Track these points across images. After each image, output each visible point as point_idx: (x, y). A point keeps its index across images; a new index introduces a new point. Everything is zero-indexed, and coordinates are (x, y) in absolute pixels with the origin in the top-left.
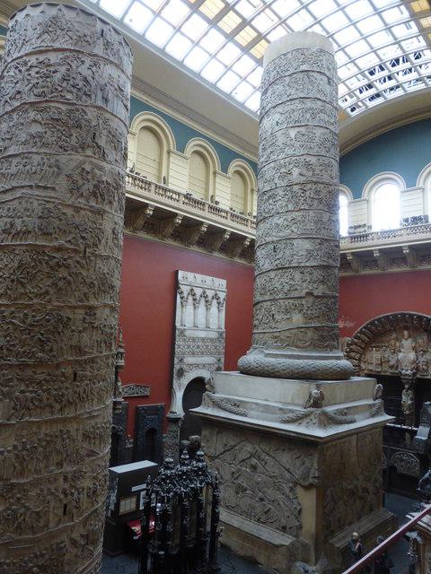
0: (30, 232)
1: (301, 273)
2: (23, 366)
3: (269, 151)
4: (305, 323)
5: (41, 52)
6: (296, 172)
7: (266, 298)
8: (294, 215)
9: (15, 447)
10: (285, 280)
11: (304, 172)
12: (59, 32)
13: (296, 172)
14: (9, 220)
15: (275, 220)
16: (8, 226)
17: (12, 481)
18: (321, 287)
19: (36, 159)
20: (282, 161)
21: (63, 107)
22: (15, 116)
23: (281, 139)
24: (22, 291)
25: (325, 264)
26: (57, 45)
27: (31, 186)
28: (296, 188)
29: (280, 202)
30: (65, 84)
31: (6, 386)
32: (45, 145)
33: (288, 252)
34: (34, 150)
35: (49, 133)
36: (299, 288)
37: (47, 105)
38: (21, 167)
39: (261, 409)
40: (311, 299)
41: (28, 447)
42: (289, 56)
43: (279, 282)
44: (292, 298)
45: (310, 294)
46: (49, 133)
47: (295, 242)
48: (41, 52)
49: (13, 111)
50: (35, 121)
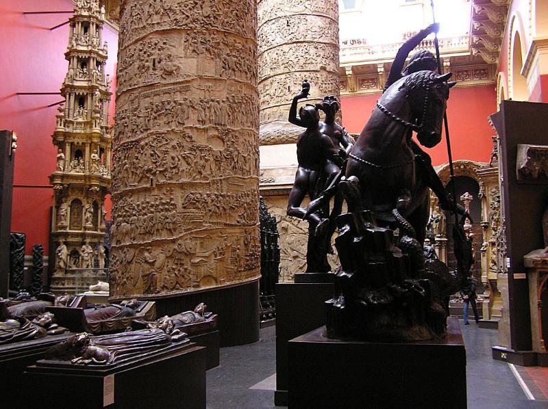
1: (316, 48)
9: (227, 98)
10: (300, 53)
17: (229, 127)
18: (332, 64)
33: (302, 28)
36: (314, 61)
40: (324, 74)
41: (237, 101)
43: (293, 54)
44: (308, 71)
45: (323, 68)
47: (308, 17)
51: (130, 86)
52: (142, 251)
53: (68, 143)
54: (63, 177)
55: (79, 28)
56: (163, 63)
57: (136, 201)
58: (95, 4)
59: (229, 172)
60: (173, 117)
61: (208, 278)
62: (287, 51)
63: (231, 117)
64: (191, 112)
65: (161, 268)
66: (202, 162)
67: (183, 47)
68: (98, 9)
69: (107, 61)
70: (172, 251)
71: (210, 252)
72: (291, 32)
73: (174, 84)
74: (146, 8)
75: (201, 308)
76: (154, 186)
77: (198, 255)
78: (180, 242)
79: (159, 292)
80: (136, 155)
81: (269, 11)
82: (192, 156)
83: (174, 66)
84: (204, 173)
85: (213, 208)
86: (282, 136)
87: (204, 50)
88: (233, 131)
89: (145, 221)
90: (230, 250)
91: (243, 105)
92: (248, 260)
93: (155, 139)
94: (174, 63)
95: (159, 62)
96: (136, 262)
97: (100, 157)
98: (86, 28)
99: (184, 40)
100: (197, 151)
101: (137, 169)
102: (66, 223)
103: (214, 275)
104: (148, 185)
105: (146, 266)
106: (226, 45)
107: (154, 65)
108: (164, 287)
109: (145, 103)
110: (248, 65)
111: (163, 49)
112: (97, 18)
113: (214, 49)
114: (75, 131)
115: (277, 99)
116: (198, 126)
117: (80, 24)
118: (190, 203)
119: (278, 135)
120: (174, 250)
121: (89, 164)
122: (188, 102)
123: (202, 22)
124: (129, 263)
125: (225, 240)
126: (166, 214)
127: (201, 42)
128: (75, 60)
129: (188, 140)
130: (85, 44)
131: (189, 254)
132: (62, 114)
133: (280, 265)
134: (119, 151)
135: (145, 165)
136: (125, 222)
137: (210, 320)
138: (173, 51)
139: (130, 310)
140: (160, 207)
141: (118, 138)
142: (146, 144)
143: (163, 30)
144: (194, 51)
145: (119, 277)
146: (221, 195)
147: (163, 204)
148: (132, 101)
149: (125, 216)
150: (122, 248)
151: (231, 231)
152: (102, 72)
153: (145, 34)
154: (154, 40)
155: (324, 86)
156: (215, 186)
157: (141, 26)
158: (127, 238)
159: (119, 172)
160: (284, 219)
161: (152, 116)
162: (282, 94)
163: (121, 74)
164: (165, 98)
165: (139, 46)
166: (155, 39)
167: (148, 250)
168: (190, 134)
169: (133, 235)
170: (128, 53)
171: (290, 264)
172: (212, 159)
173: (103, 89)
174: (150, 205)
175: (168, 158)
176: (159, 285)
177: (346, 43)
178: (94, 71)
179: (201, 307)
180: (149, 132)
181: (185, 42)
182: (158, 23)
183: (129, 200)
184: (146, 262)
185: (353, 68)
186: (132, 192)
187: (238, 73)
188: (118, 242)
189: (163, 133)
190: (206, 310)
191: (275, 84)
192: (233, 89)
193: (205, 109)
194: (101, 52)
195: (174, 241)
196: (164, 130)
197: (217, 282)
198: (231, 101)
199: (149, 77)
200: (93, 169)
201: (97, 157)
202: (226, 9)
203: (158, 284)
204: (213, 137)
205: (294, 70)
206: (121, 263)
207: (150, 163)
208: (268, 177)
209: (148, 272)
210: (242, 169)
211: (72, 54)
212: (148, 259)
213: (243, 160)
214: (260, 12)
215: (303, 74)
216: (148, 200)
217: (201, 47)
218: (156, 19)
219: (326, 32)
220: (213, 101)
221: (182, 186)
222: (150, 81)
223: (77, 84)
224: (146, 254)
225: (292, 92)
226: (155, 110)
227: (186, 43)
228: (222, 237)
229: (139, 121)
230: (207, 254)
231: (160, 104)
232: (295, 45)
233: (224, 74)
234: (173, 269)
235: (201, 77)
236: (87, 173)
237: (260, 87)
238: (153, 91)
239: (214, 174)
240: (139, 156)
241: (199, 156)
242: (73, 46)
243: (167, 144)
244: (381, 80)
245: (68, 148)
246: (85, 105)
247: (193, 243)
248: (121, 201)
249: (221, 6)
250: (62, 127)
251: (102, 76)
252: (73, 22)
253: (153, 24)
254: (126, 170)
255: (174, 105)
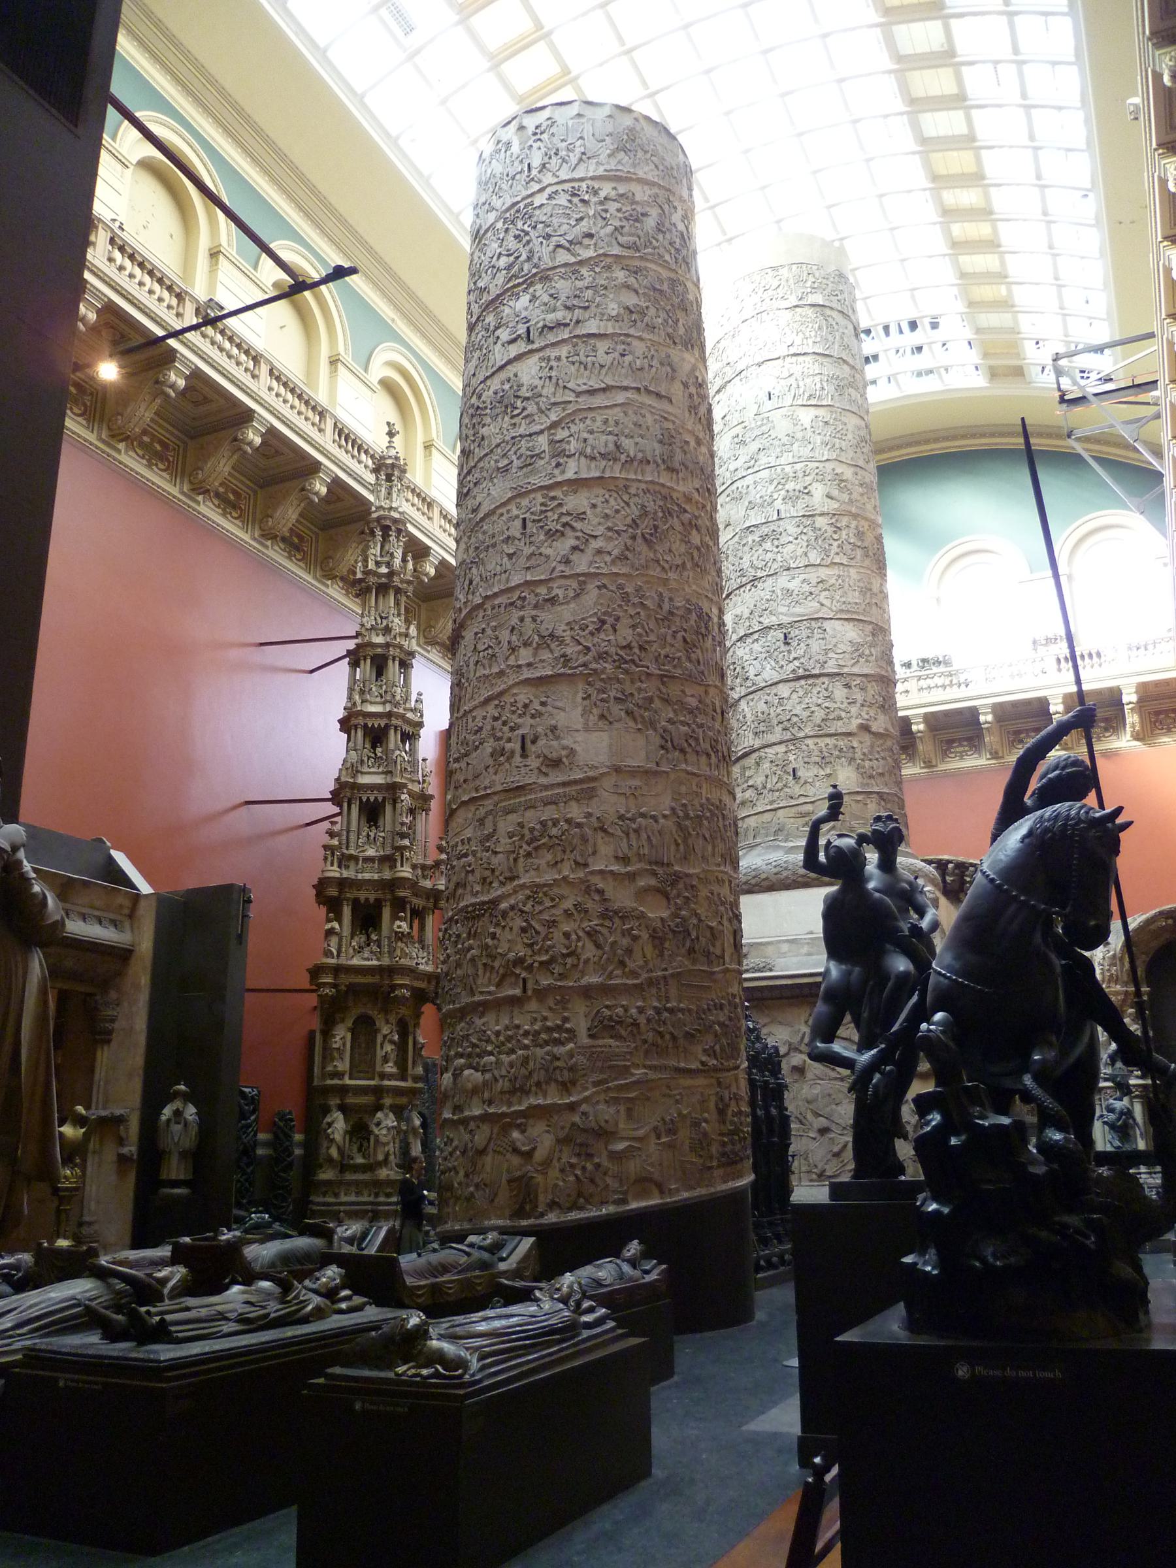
0: (648, 462)
1: (847, 686)
2: (664, 678)
3: (754, 447)
4: (863, 785)
5: (618, 179)
6: (818, 490)
7: (771, 738)
8: (823, 573)
9: (673, 809)
10: (813, 699)
11: (835, 493)
12: (640, 154)
13: (818, 490)
14: (610, 437)
15: (783, 581)
16: (611, 447)
17: (677, 868)
18: (881, 717)
19: (639, 348)
20: (788, 469)
21: (665, 274)
22: (584, 271)
23: (782, 427)
24: (652, 555)
25: (883, 673)
26: (641, 174)
27: (638, 389)
28: (821, 522)
29: (791, 547)
30: (660, 237)
31: (646, 709)
32: (651, 328)
33: (816, 646)
34: (632, 331)
35: (652, 312)
36: (843, 714)
37: (643, 264)
38: (616, 355)
39: (805, 950)
40: (867, 738)
41: (692, 814)
42: (784, 272)
45: (865, 728)
46: (652, 312)
47: (827, 625)
48: (618, 179)
49: (581, 263)
50: (628, 287)
51: (477, 790)
52: (505, 1129)
53: (348, 899)
54: (337, 970)
55: (366, 666)
56: (541, 742)
57: (494, 1023)
58: (396, 620)
59: (681, 962)
60: (564, 852)
61: (644, 1183)
62: (786, 695)
63: (682, 847)
64: (600, 841)
65: (547, 1163)
66: (625, 942)
67: (580, 709)
68: (403, 630)
69: (422, 732)
70: (568, 1126)
71: (647, 1128)
72: (793, 655)
73: (564, 784)
74: (505, 635)
75: (633, 1251)
76: (530, 993)
77: (624, 1134)
78: (584, 1107)
79: (542, 1215)
80: (492, 930)
81: (746, 614)
82: (605, 931)
83: (564, 748)
84: (631, 965)
85: (650, 1036)
86: (785, 874)
87: (623, 714)
88: (687, 875)
89: (511, 1065)
90: (688, 1123)
91: (705, 822)
92: (724, 1144)
93: (529, 898)
94: (564, 742)
95: (534, 742)
96: (495, 1151)
97: (411, 927)
98: (380, 667)
99: (581, 695)
100: (616, 920)
101: (493, 957)
102: (343, 1065)
103: (656, 1176)
104: (517, 991)
105: (516, 1160)
106: (666, 701)
107: (523, 748)
108: (553, 1205)
109: (507, 824)
110: (711, 738)
111: (540, 714)
112: (401, 647)
113: (642, 712)
114: (360, 876)
115: (770, 796)
116: (615, 868)
117: (368, 661)
118: (604, 1027)
119: (775, 870)
120: (573, 1124)
121: (390, 942)
122: (593, 819)
123: (616, 658)
124: (482, 1152)
125: (677, 1102)
126: (555, 1050)
127: (615, 698)
128: (360, 733)
129: (597, 898)
130: (378, 699)
131: (605, 1134)
132: (335, 842)
133: (792, 1149)
134: (457, 922)
135: (510, 950)
136: (470, 1067)
137: (653, 1276)
138: (561, 719)
139: (486, 1255)
140: (544, 1036)
141: (454, 894)
142: (512, 908)
143: (540, 678)
144: (602, 717)
145: (460, 1184)
146: (667, 1010)
147: (549, 1030)
148: (481, 821)
149: (469, 1056)
150: (465, 1122)
151: (688, 1082)
152: (413, 752)
153: (503, 686)
154: (522, 698)
155: (867, 764)
156: (654, 991)
157: (495, 670)
158: (475, 1100)
159: (458, 965)
160: (797, 1050)
161: (521, 852)
162: (780, 785)
163: (456, 765)
164: (549, 813)
165: (491, 710)
166: (523, 695)
167: (518, 1126)
168: (601, 886)
169: (486, 1095)
170: (471, 724)
171: (813, 1145)
172: (645, 935)
173: (416, 788)
174: (521, 1032)
175: (557, 935)
176: (543, 1199)
177: (908, 665)
178: (398, 752)
179: (633, 1248)
180: (516, 883)
181: (584, 699)
182: (529, 665)
183: (479, 1022)
184: (516, 1151)
185: (929, 719)
186: (483, 1008)
187: (692, 757)
188: (457, 1109)
189: (545, 885)
190: (646, 1255)
191: (766, 765)
192: (683, 789)
193: (628, 835)
194: (410, 715)
195: (572, 1107)
196: (548, 877)
197: (662, 1192)
198: (681, 814)
199: (515, 772)
200: (398, 952)
201: (404, 926)
202: (663, 630)
203: (541, 1198)
204: (647, 890)
205: (802, 734)
206: (463, 1153)
207: (520, 947)
208: (757, 961)
209: (518, 1173)
210: (708, 954)
211: (354, 721)
212: (518, 1144)
213: (708, 934)
214: (728, 618)
215: (822, 742)
216: (517, 1022)
217: (617, 710)
218: (525, 655)
219: (867, 652)
220: (643, 815)
221: (587, 993)
222: (518, 779)
223: (364, 780)
224: (516, 1134)
225: (802, 781)
226: (528, 837)
227: (587, 702)
228: (670, 1096)
229: (495, 860)
230: (641, 1133)
231: (538, 827)
232: (803, 682)
233: (664, 760)
234: (572, 1166)
235: (617, 770)
236: (386, 961)
237: (736, 769)
238: (522, 799)
239: (651, 966)
240: (498, 931)
241: (619, 931)
242: (355, 704)
243: (553, 907)
244: (987, 739)
245: (347, 911)
246: (381, 823)
247: (612, 1110)
248: (463, 1024)
249: (652, 624)
250: (335, 867)
251: (414, 762)
252: (354, 658)
253: (519, 666)
254: (473, 960)
255: (566, 827)
